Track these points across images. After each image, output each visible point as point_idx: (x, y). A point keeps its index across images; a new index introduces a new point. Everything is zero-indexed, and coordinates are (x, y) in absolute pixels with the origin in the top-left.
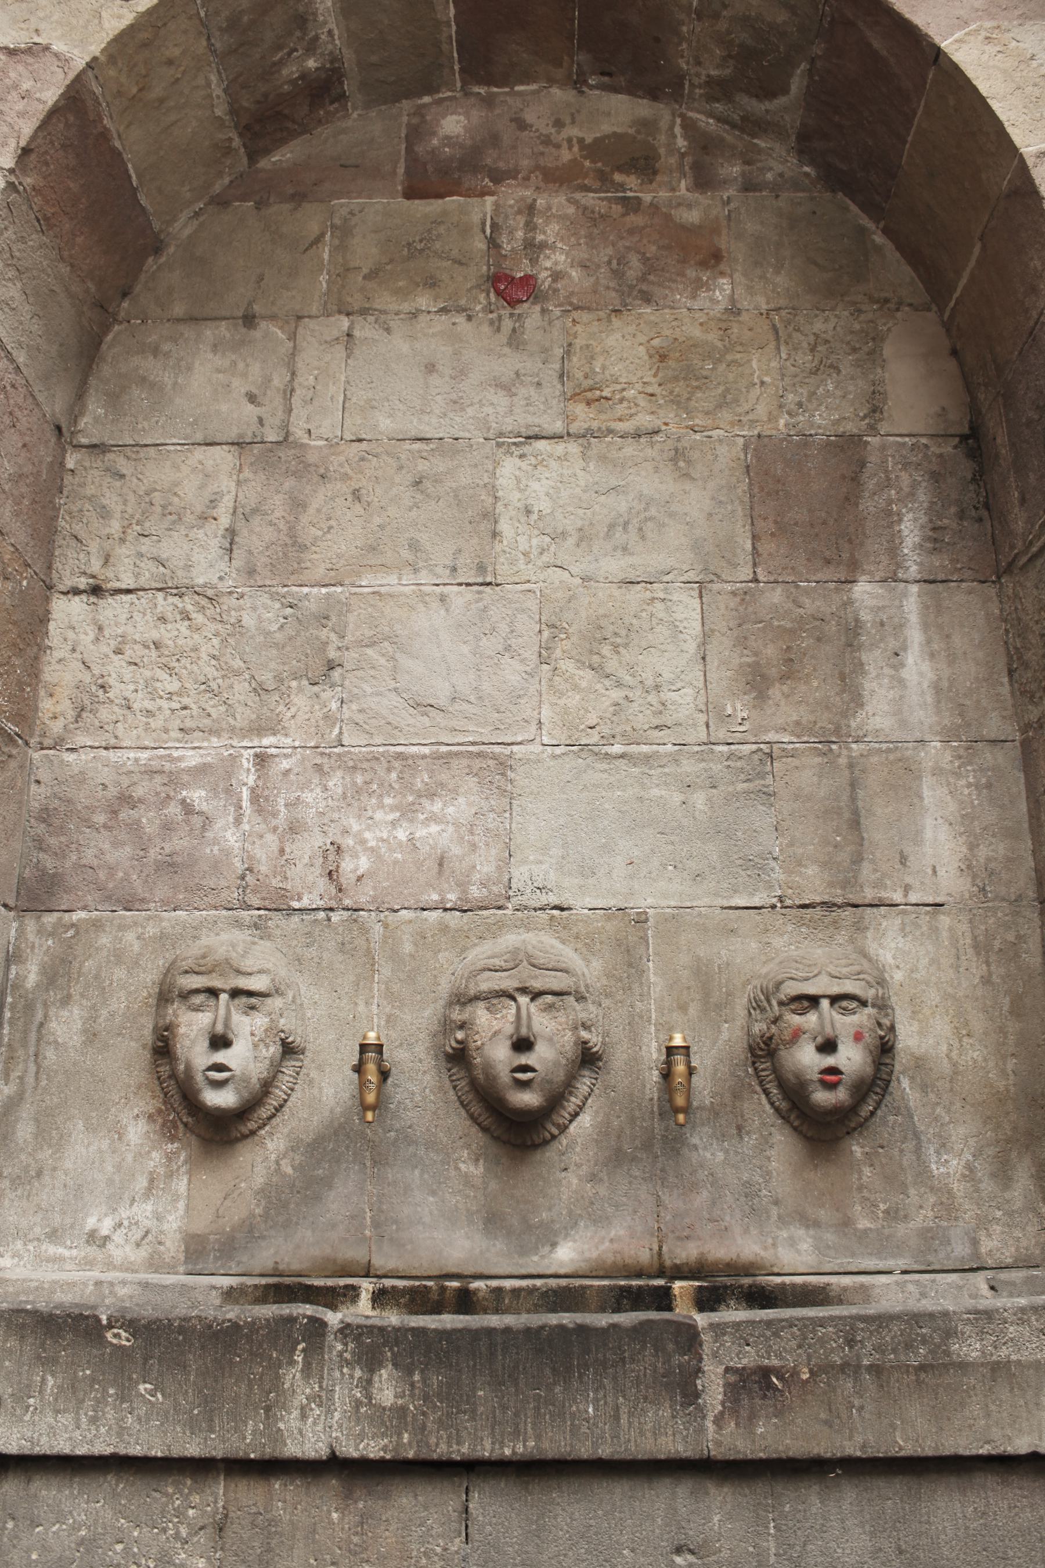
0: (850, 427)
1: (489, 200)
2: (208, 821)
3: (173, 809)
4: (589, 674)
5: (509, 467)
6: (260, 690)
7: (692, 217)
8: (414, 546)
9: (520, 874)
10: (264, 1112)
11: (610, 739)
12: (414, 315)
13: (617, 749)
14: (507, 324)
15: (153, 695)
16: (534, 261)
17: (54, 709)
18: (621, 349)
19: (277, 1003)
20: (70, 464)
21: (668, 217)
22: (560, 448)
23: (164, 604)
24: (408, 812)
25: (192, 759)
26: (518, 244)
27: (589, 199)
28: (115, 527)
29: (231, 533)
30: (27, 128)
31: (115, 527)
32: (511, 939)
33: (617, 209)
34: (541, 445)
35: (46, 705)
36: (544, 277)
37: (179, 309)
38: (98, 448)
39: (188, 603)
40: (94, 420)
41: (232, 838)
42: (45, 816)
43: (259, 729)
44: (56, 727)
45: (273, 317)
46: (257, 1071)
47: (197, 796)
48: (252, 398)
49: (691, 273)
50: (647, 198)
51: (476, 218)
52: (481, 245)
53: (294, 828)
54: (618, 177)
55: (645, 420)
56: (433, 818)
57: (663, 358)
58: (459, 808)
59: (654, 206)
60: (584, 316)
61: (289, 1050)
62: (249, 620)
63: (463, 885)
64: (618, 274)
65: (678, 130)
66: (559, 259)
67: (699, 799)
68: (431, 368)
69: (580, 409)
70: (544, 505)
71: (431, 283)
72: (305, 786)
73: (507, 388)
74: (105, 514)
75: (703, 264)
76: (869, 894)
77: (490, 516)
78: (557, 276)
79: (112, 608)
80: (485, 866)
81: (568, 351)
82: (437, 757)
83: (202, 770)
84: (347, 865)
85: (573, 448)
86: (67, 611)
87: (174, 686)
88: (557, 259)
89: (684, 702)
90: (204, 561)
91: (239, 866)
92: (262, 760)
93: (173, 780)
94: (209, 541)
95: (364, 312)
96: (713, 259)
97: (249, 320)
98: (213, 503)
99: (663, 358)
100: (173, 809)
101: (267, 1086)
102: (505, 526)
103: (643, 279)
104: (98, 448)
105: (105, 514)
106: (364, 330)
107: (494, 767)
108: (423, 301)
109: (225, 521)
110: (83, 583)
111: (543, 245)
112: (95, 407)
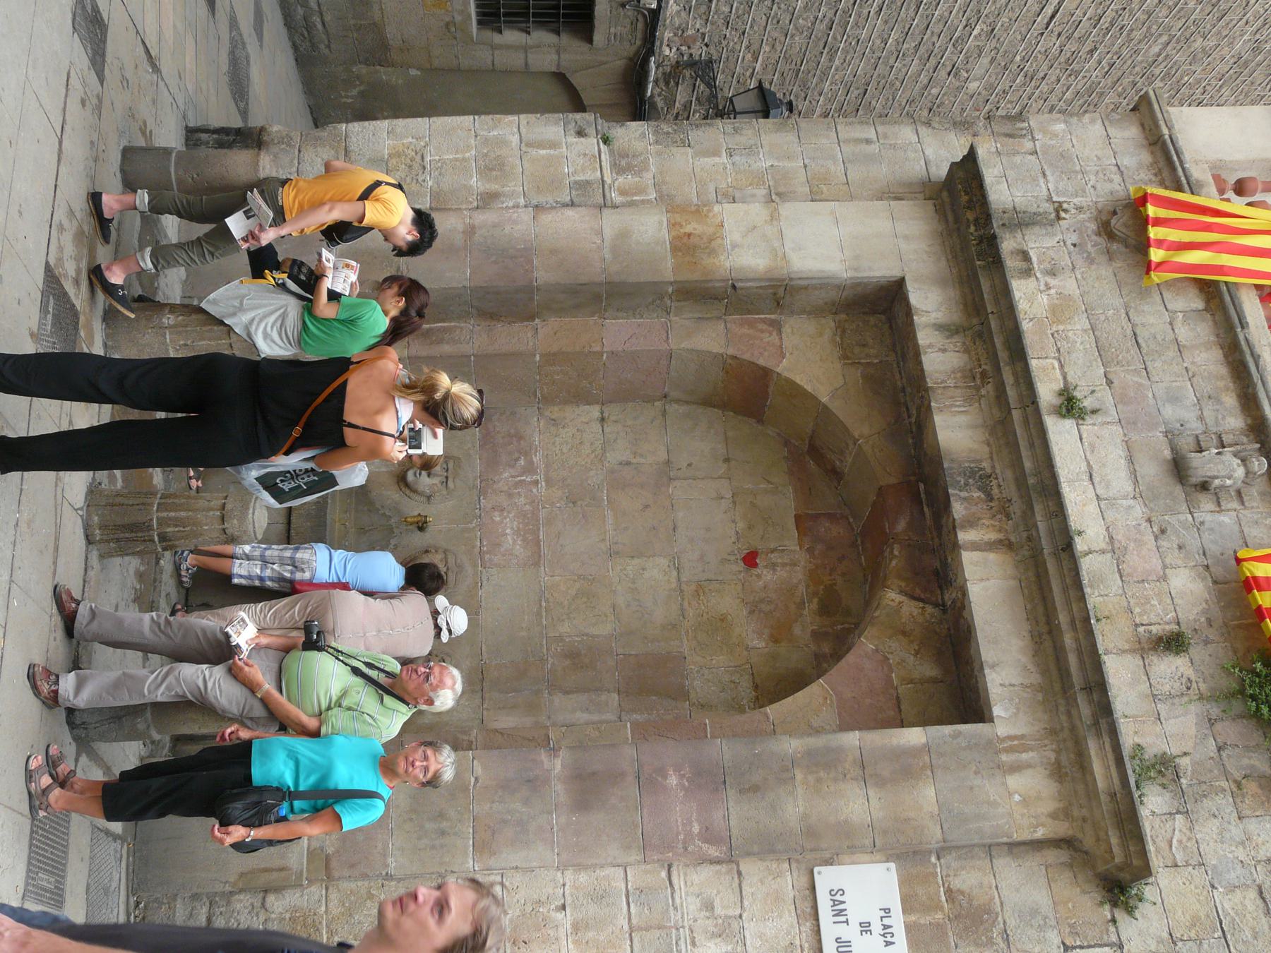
0: (692, 695)
1: (798, 548)
2: (513, 467)
3: (516, 455)
4: (574, 592)
5: (663, 562)
6: (564, 480)
7: (797, 630)
8: (626, 529)
9: (494, 571)
10: (408, 492)
11: (547, 601)
12: (733, 521)
13: (544, 604)
14: (733, 558)
15: (561, 444)
16: (766, 567)
17: (554, 411)
18: (727, 603)
19: (445, 492)
20: (657, 404)
21: (796, 621)
22: (674, 580)
23: (598, 444)
24: (517, 532)
25: (537, 459)
26: (774, 560)
27: (802, 588)
28: (630, 423)
29: (628, 463)
30: (747, 357)
31: (630, 423)
32: (469, 570)
33: (798, 600)
34: (675, 573)
35: (556, 409)
36: (755, 571)
37: (730, 434)
38: (664, 413)
39: (599, 451)
40: (673, 409)
41: (506, 475)
42: (513, 413)
43: (549, 482)
44: (547, 413)
45: (729, 469)
46: (420, 488)
47: (522, 462)
48: (690, 465)
49: (766, 631)
50: (805, 612)
51: (786, 543)
52: (772, 546)
53: (510, 495)
54: (816, 600)
55: (690, 613)
56: (514, 541)
57: (722, 620)
58: (519, 549)
59: (801, 615)
60: (739, 587)
61: (429, 498)
62: (592, 473)
63: (488, 552)
64: (762, 601)
65: (847, 626)
66: (765, 576)
67: (524, 633)
68: (708, 529)
69: (693, 587)
70: (647, 575)
71: (750, 527)
72: (526, 497)
73: (701, 558)
74: (635, 418)
75: (771, 636)
76: (487, 695)
77: (641, 555)
78: (759, 576)
79: (596, 427)
80: (496, 559)
81: (721, 582)
82: (538, 542)
83: (531, 462)
84: (496, 513)
85: (674, 585)
86: (595, 411)
87: (565, 450)
88: (768, 576)
89: (565, 628)
90: (614, 457)
91: (496, 479)
92: (536, 483)
93: (526, 454)
94: (625, 455)
95: (734, 502)
96: (775, 640)
97: (727, 460)
98: (641, 456)
99: (722, 620)
100: (516, 455)
101: (415, 491)
102: (636, 561)
103: (760, 611)
104: (664, 413)
105: (635, 418)
106: (725, 504)
107: (536, 560)
108: (741, 525)
109: (634, 461)
110: (606, 415)
111: (774, 570)
112: (682, 409)
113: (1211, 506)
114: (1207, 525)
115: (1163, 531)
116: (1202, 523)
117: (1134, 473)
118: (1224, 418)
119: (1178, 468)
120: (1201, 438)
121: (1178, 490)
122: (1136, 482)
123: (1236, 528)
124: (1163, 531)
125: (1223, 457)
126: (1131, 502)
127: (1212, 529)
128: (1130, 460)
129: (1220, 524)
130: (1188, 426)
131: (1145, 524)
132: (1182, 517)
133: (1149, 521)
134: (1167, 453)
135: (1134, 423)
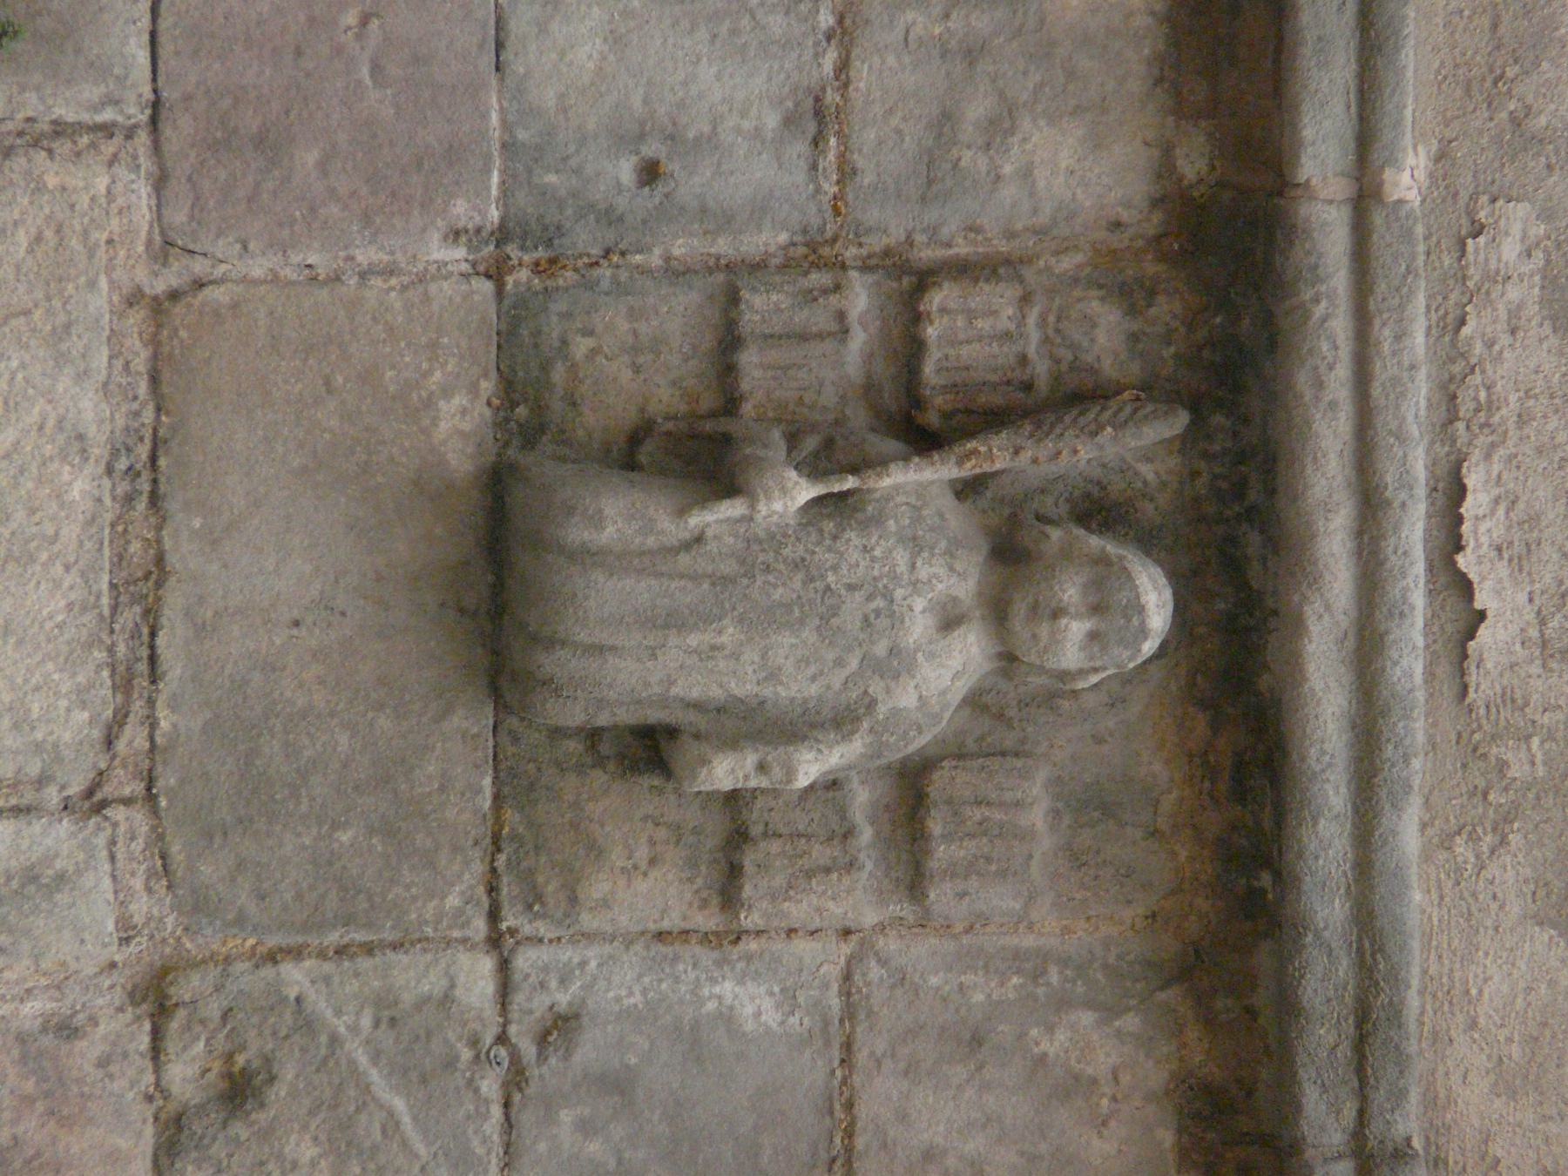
113: (662, 893)
114: (589, 1050)
115: (239, 1091)
116: (560, 1028)
117: (144, 586)
118: (999, 129)
119: (491, 581)
120: (762, 306)
121: (455, 757)
122: (139, 672)
123: (813, 1071)
124: (239, 1091)
125: (852, 555)
126: (56, 838)
127: (617, 1085)
128: (149, 473)
129: (696, 1040)
130: (691, 182)
131: (116, 1025)
132: (414, 977)
133: (155, 997)
134: (459, 422)
135: (270, 145)
